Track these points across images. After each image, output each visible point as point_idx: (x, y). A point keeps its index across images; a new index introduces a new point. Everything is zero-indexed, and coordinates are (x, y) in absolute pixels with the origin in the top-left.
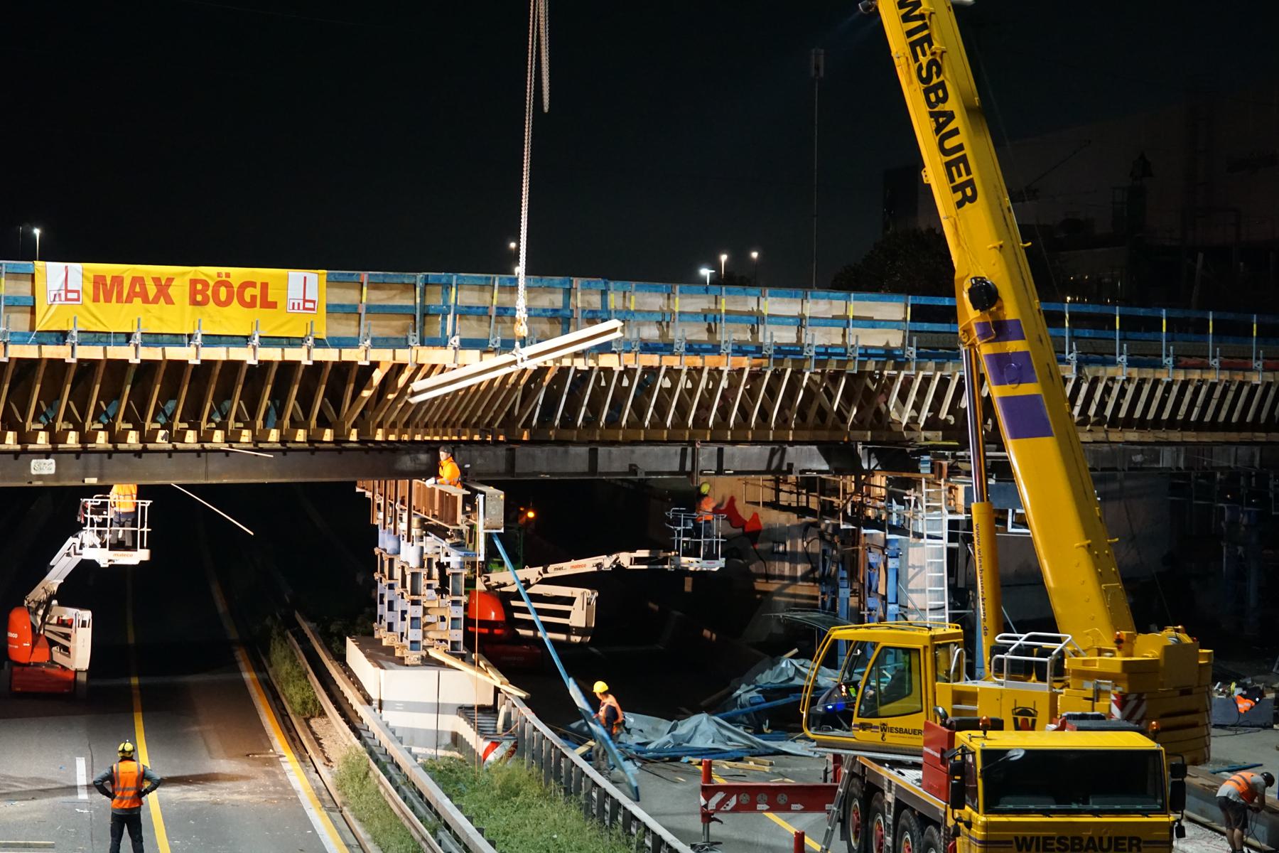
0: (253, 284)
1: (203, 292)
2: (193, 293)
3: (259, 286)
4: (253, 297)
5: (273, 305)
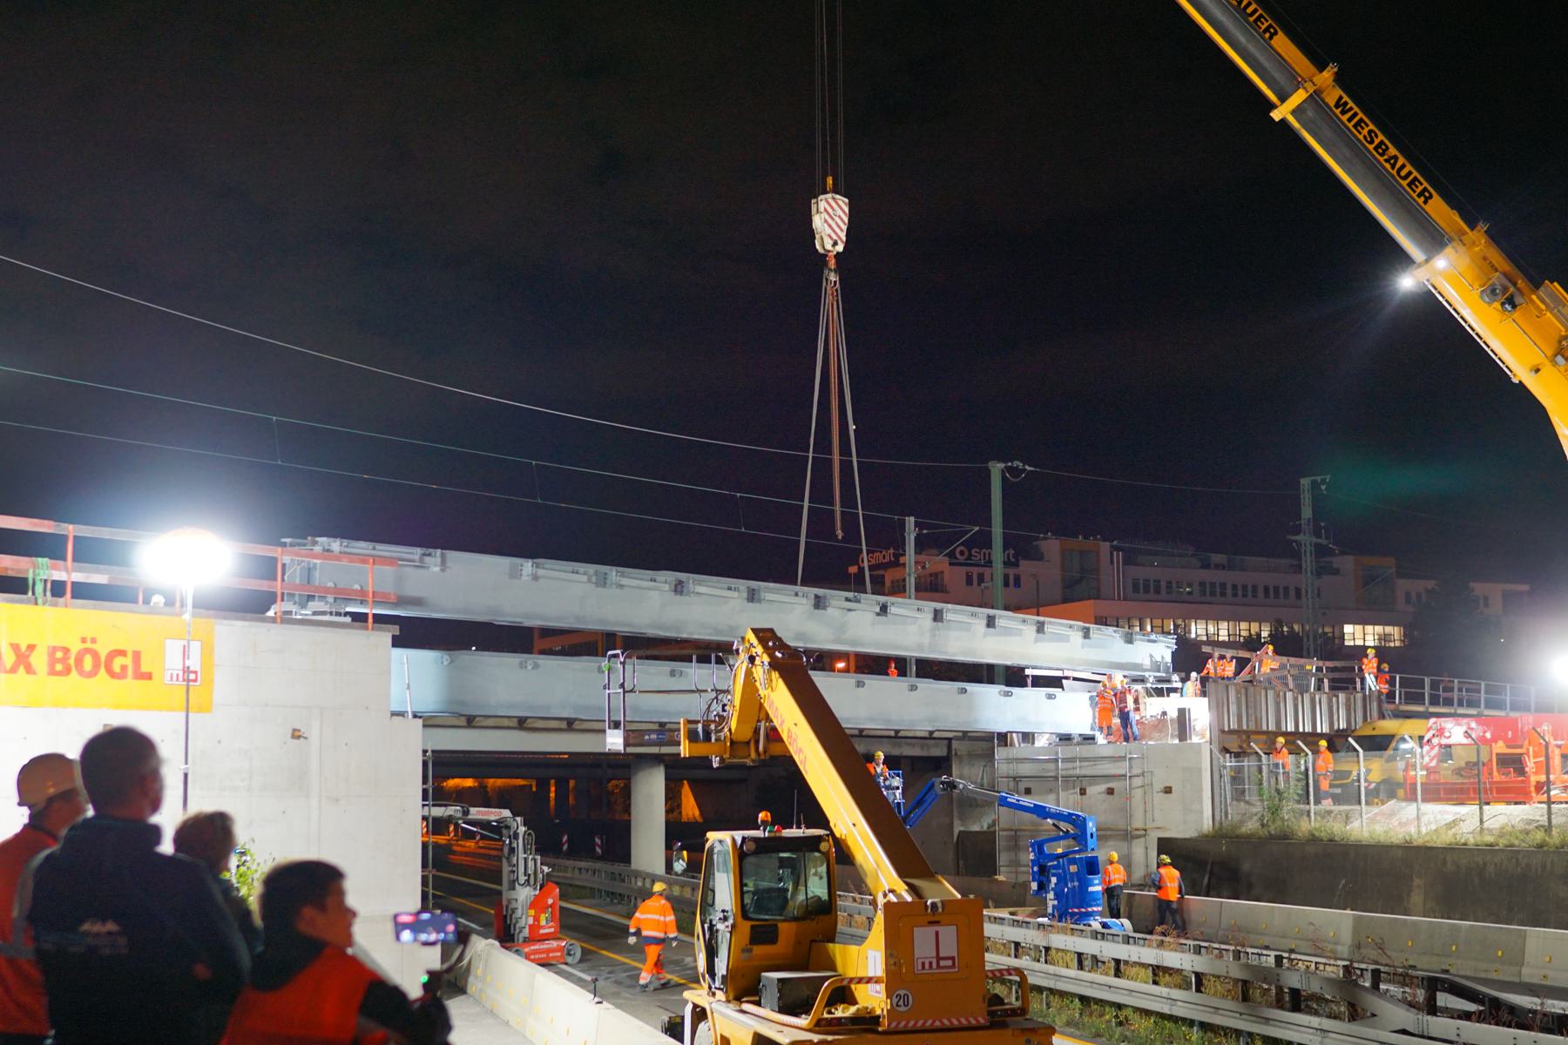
0: (122, 653)
1: (64, 660)
2: (52, 661)
3: (130, 655)
4: (124, 668)
5: (148, 676)
